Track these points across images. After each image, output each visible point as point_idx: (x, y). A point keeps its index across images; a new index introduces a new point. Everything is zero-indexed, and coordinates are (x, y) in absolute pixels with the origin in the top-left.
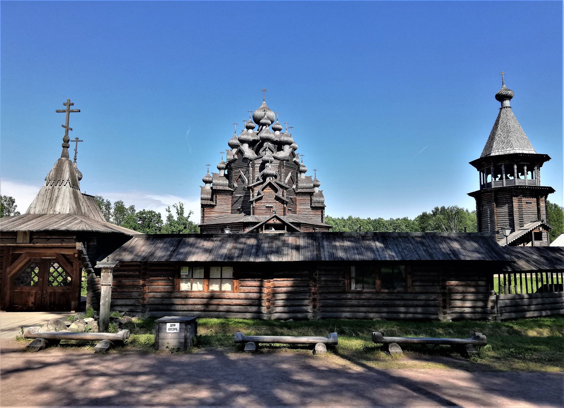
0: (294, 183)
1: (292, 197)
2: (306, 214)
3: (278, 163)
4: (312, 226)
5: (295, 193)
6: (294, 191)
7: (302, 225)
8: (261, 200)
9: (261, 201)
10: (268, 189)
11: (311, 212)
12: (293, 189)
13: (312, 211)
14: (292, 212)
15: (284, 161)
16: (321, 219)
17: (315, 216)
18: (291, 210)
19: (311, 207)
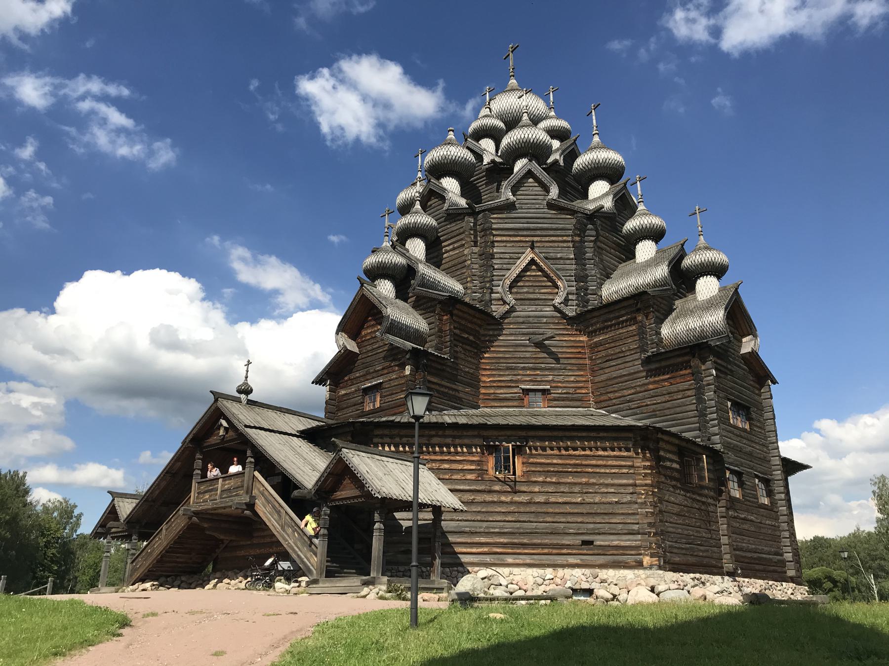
0: (557, 287)
1: (541, 338)
2: (628, 398)
3: (462, 230)
4: (479, 436)
5: (571, 320)
6: (564, 316)
7: (377, 436)
8: (351, 372)
9: (352, 376)
10: (373, 326)
11: (651, 387)
12: (557, 309)
13: (652, 380)
14: (555, 400)
15: (480, 216)
16: (693, 407)
17: (667, 397)
18: (544, 392)
19: (647, 361)
